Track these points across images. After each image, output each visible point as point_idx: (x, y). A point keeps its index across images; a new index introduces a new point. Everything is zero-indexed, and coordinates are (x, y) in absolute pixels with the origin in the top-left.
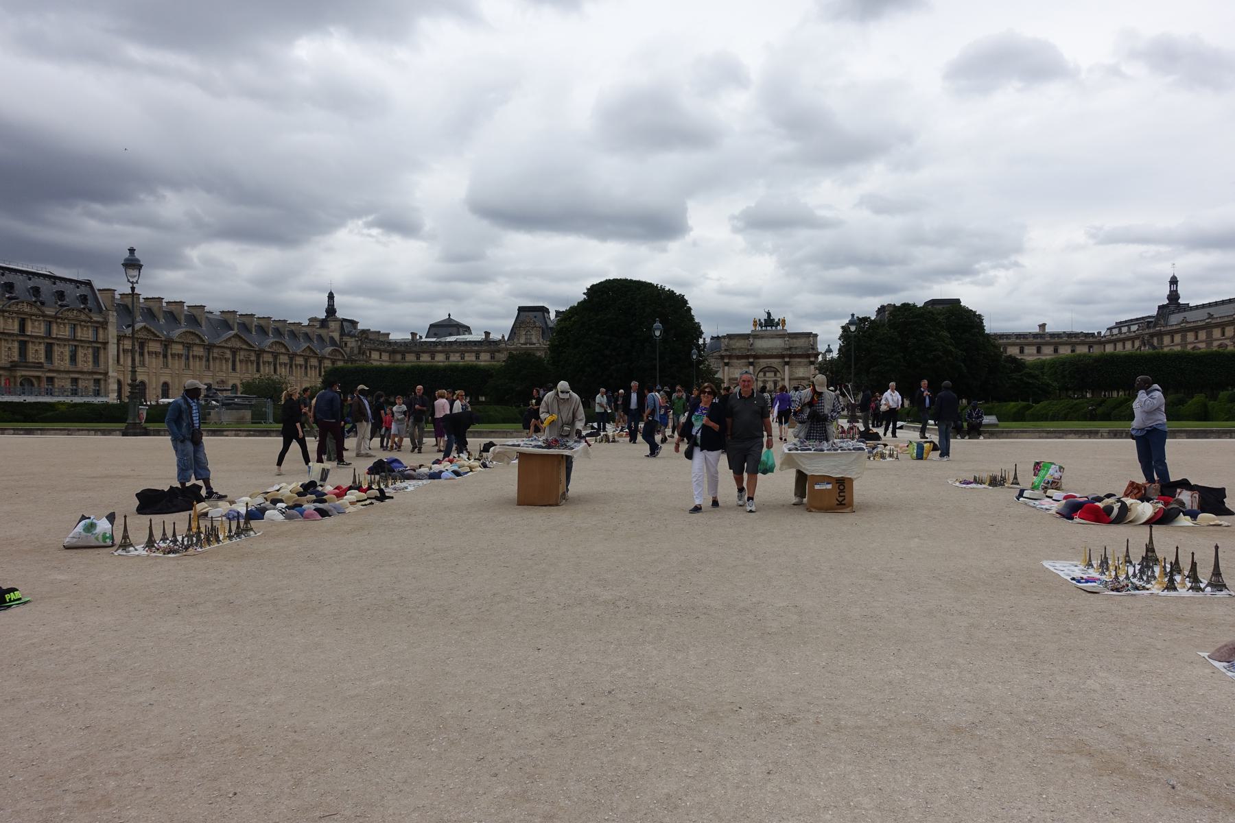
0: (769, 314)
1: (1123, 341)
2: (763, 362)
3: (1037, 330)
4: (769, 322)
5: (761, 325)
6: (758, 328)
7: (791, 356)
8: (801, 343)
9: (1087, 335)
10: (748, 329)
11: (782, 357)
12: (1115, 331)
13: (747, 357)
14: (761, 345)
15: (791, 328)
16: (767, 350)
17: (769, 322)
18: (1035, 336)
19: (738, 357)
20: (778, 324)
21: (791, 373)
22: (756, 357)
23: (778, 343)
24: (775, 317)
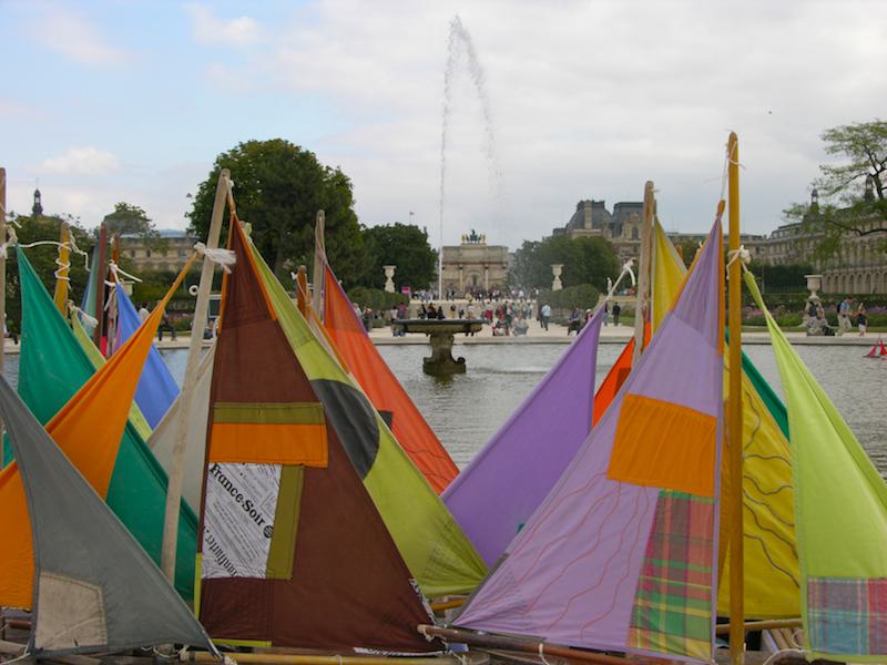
1: (780, 244)
2: (469, 267)
4: (474, 237)
6: (466, 242)
7: (489, 263)
9: (755, 237)
10: (458, 243)
11: (483, 263)
12: (775, 235)
13: (458, 263)
14: (467, 254)
15: (490, 242)
17: (474, 237)
19: (451, 264)
21: (490, 275)
22: (464, 263)
24: (478, 234)
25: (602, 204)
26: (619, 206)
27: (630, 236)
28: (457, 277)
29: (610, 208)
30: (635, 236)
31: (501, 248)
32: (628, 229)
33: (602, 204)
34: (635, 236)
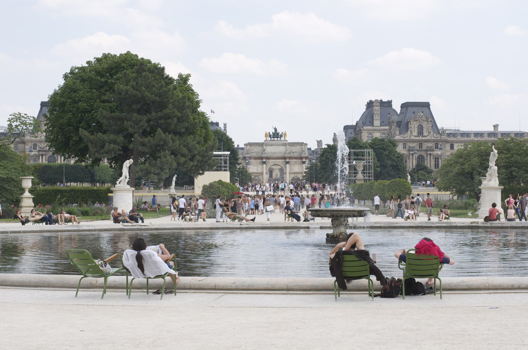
0: (276, 130)
2: (272, 162)
3: (492, 129)
4: (276, 135)
5: (270, 136)
6: (269, 139)
7: (290, 158)
8: (297, 149)
10: (261, 139)
11: (285, 158)
13: (262, 158)
14: (270, 150)
15: (290, 139)
16: (275, 153)
17: (276, 135)
18: (490, 134)
19: (256, 158)
20: (281, 136)
21: (290, 170)
22: (267, 158)
23: (282, 149)
24: (280, 131)
25: (389, 103)
26: (404, 106)
27: (415, 133)
28: (260, 171)
29: (397, 107)
30: (420, 132)
31: (302, 144)
32: (414, 126)
33: (389, 103)
34: (420, 132)
